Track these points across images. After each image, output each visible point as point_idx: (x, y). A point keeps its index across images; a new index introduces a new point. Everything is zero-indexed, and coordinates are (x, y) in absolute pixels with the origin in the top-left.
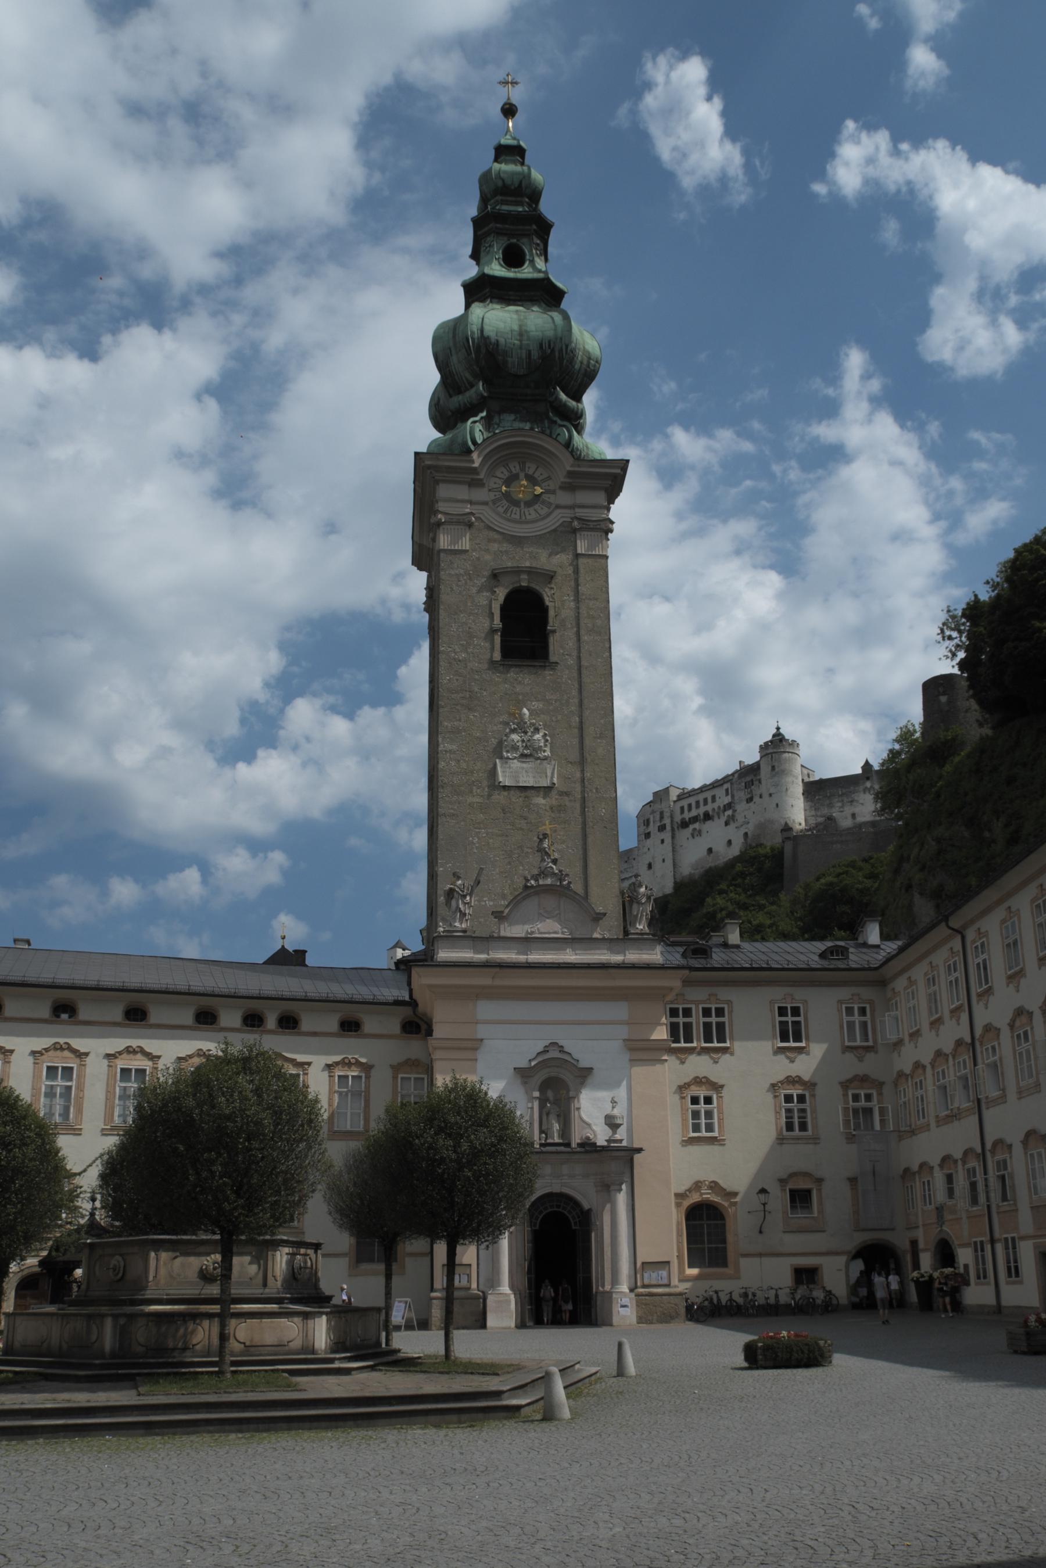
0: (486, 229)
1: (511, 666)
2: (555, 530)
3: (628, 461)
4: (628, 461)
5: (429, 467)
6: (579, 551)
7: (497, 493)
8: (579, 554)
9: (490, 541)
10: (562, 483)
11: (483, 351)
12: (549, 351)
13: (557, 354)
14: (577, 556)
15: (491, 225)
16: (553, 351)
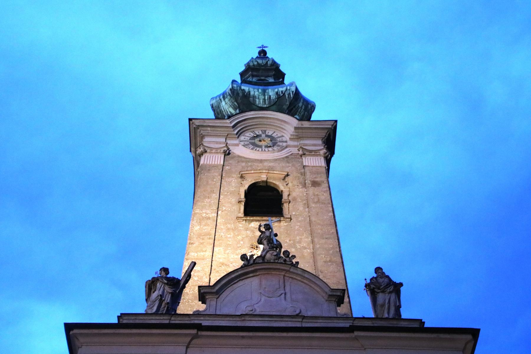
0: (247, 76)
1: (252, 221)
2: (287, 157)
3: (336, 121)
4: (336, 121)
5: (198, 127)
6: (304, 164)
7: (244, 142)
8: (306, 166)
9: (238, 162)
10: (291, 135)
11: (241, 94)
12: (282, 95)
13: (287, 96)
14: (304, 167)
15: (250, 73)
16: (284, 94)
